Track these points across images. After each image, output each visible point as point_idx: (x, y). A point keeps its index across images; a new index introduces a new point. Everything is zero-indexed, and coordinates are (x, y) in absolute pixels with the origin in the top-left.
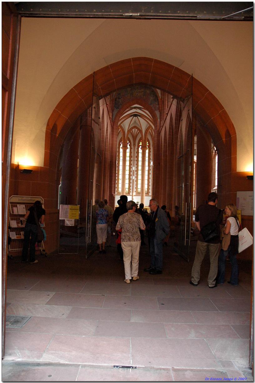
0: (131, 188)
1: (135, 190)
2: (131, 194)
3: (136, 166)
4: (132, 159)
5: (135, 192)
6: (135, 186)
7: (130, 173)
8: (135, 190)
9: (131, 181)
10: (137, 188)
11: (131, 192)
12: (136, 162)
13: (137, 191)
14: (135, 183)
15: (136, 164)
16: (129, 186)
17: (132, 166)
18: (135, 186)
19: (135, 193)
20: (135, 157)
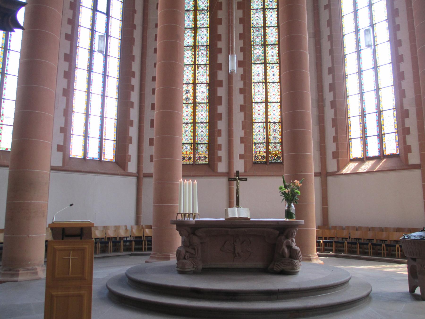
0: (222, 140)
1: (239, 149)
2: (222, 167)
3: (241, 42)
4: (221, 14)
5: (241, 157)
6: (238, 132)
7: (212, 75)
8: (239, 149)
9: (222, 109)
10: (248, 140)
11: (220, 159)
12: (238, 44)
13: (248, 154)
14: (238, 117)
15: (242, 36)
16: (213, 132)
17: (221, 58)
18: (238, 132)
19: (242, 161)
20: (235, 6)
